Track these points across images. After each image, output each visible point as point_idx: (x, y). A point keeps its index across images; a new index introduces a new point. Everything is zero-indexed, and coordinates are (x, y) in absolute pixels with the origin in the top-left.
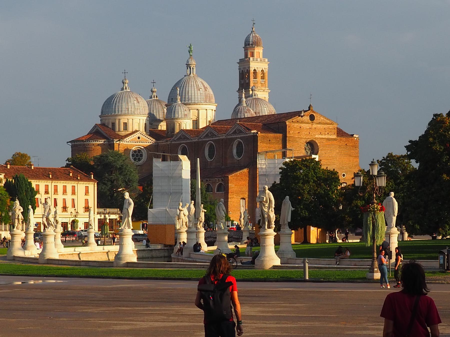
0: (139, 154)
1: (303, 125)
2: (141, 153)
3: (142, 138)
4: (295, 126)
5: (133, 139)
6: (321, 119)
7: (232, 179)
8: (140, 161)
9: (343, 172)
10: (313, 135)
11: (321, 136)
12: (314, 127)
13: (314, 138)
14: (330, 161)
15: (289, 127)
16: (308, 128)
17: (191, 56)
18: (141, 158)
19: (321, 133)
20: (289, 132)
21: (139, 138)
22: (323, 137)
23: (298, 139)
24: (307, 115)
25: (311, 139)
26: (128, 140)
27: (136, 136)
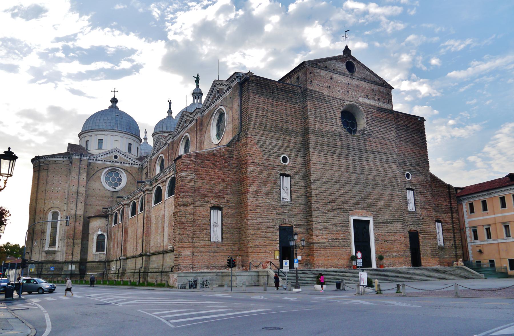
0: (116, 178)
1: (335, 76)
2: (119, 177)
3: (121, 158)
4: (322, 74)
5: (106, 158)
6: (366, 73)
7: (189, 162)
8: (118, 187)
9: (407, 171)
10: (354, 96)
11: (367, 101)
12: (356, 83)
13: (357, 101)
14: (386, 147)
15: (311, 73)
16: (346, 84)
17: (198, 86)
18: (119, 183)
19: (367, 96)
20: (311, 81)
21: (116, 157)
22: (372, 103)
23: (328, 99)
24: (343, 61)
25: (351, 103)
26: (99, 158)
27: (111, 154)
